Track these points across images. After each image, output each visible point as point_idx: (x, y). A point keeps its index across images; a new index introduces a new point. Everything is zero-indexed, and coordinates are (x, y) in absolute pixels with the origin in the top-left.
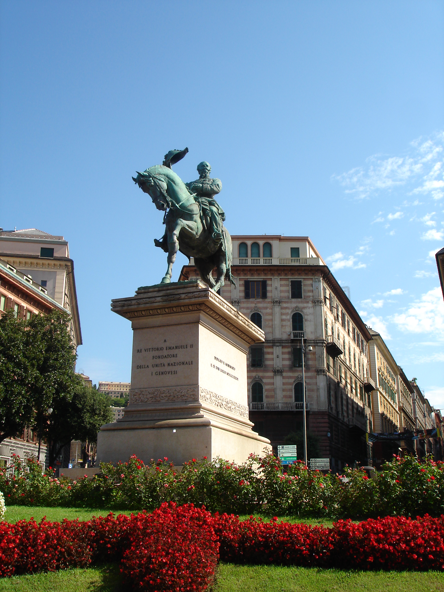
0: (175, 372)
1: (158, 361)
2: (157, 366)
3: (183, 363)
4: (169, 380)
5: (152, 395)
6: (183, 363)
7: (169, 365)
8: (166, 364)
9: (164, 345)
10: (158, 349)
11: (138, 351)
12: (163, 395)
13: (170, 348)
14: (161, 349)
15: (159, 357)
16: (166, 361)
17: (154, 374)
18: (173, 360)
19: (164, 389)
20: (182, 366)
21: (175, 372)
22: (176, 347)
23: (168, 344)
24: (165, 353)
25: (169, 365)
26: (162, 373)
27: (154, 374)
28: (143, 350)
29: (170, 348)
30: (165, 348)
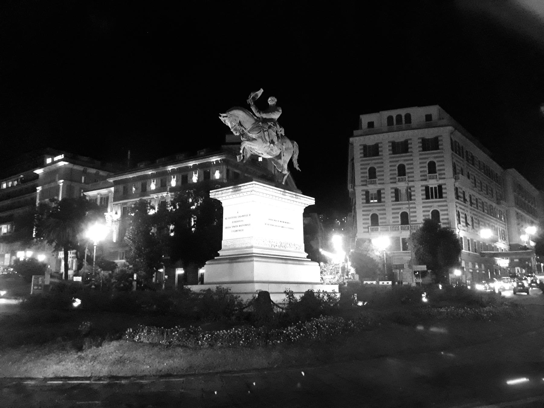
0: (243, 230)
1: (235, 224)
7: (239, 226)
8: (238, 226)
16: (238, 224)
21: (243, 230)
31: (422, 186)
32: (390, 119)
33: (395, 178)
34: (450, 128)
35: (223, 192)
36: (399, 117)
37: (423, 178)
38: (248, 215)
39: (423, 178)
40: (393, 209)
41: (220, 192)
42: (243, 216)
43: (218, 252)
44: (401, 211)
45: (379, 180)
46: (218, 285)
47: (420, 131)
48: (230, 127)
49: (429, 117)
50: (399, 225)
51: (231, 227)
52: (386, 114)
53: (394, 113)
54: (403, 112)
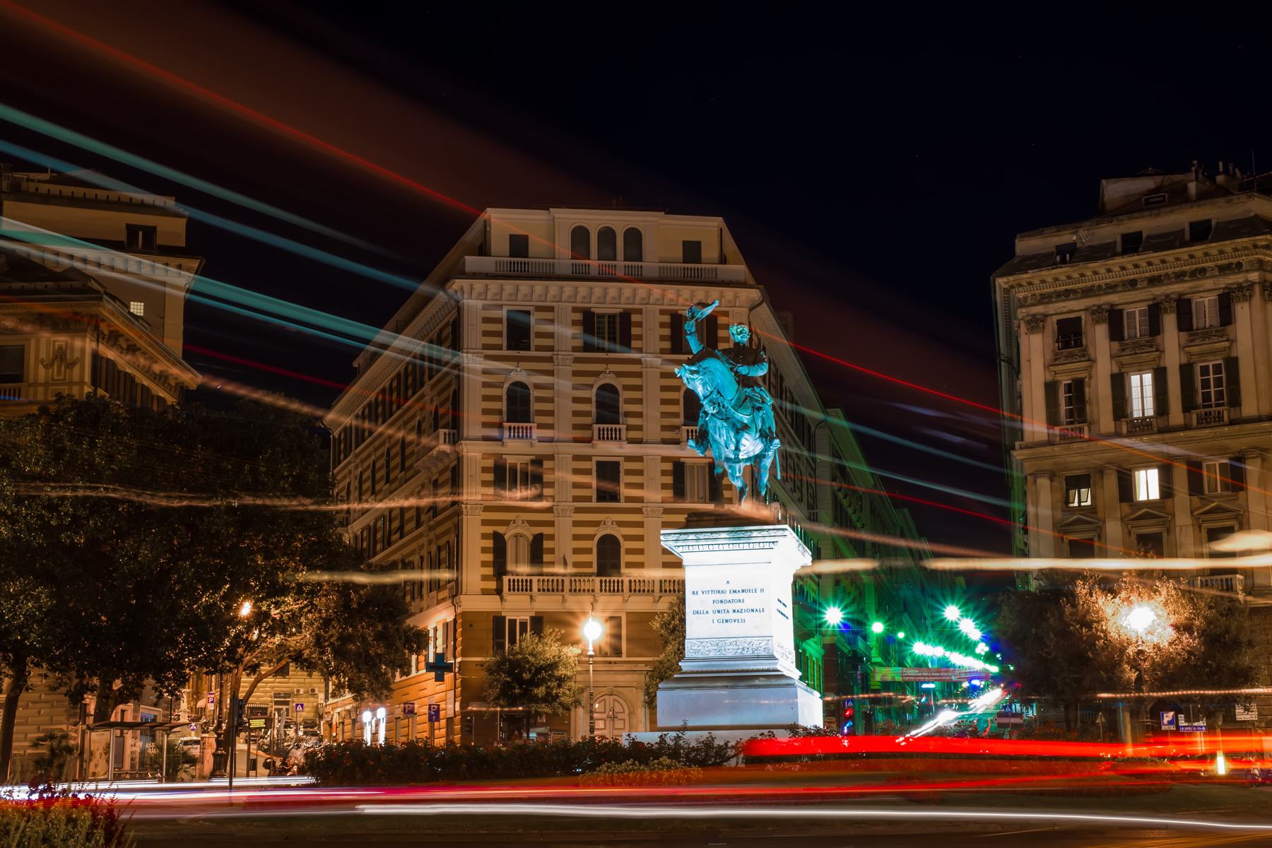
2: (719, 612)
3: (753, 611)
4: (733, 630)
5: (715, 648)
6: (753, 611)
7: (734, 611)
8: (731, 611)
9: (727, 588)
10: (719, 592)
11: (693, 593)
12: (729, 647)
13: (735, 592)
14: (723, 592)
15: (722, 602)
16: (730, 607)
17: (715, 621)
18: (738, 606)
19: (731, 640)
20: (751, 613)
22: (743, 591)
23: (732, 586)
24: (729, 596)
25: (734, 611)
26: (727, 621)
27: (715, 621)
28: (700, 593)
29: (735, 592)
30: (728, 592)
31: (665, 459)
32: (580, 236)
33: (588, 427)
34: (754, 294)
35: (701, 536)
36: (607, 235)
37: (668, 435)
38: (758, 591)
39: (668, 435)
40: (576, 524)
41: (691, 537)
42: (743, 591)
43: (680, 664)
44: (600, 532)
45: (540, 426)
46: (705, 734)
47: (671, 291)
48: (701, 395)
49: (692, 251)
50: (591, 575)
51: (710, 612)
52: (568, 218)
53: (595, 220)
54: (620, 220)
